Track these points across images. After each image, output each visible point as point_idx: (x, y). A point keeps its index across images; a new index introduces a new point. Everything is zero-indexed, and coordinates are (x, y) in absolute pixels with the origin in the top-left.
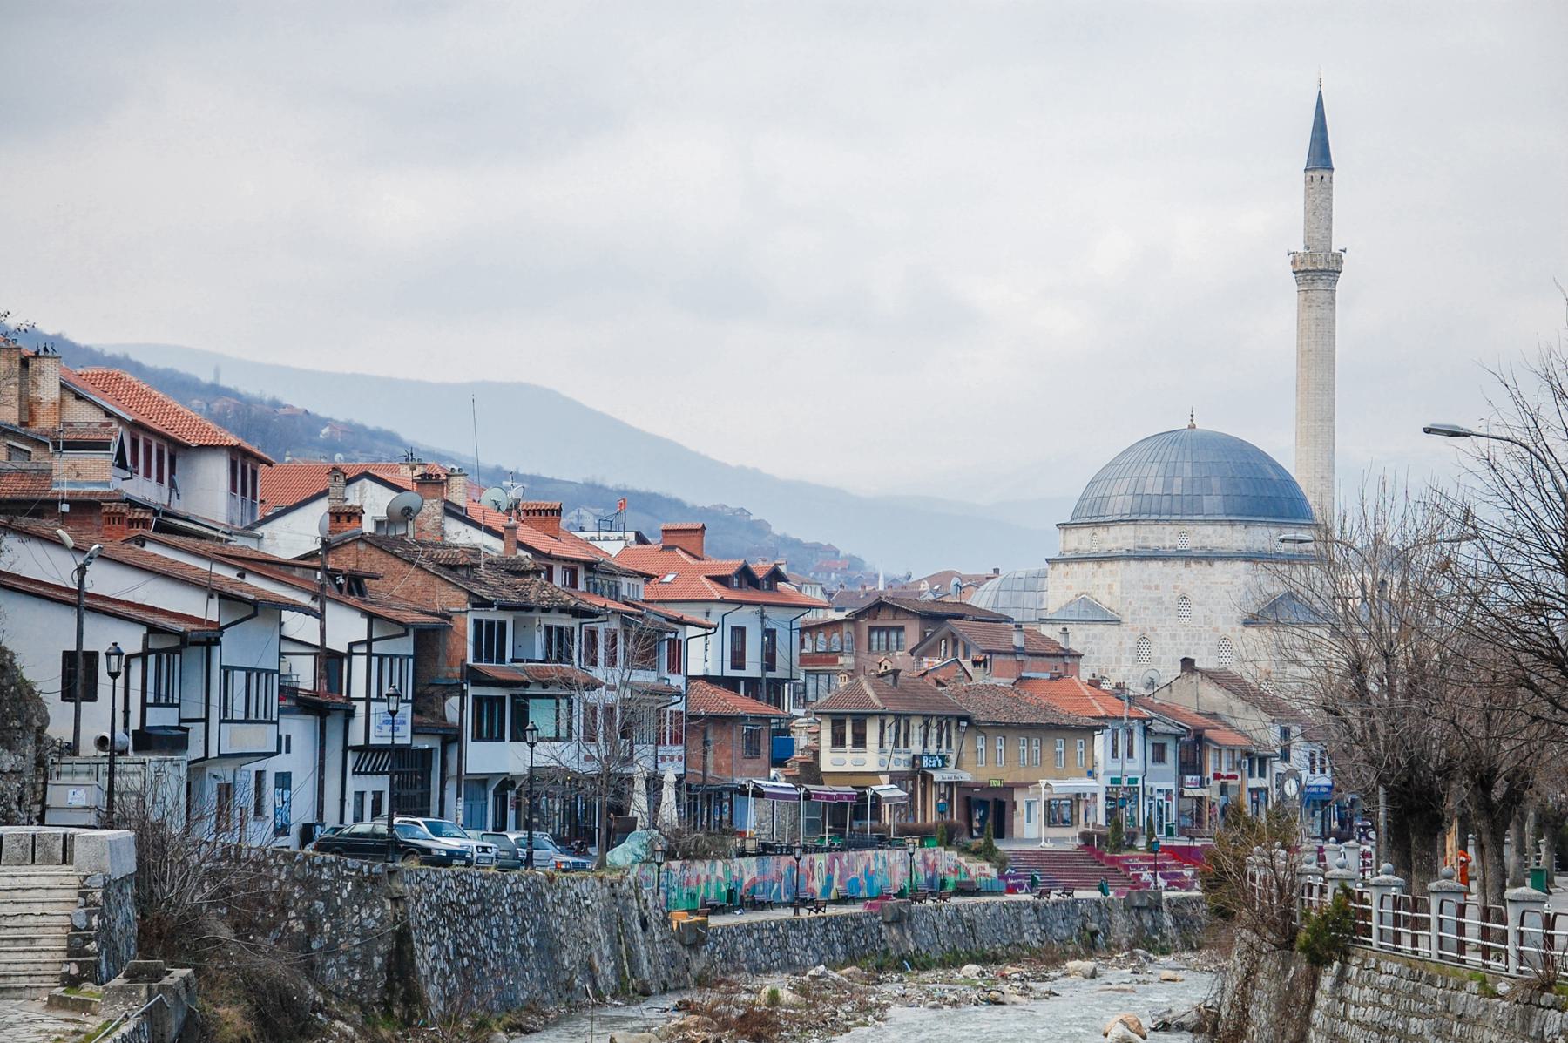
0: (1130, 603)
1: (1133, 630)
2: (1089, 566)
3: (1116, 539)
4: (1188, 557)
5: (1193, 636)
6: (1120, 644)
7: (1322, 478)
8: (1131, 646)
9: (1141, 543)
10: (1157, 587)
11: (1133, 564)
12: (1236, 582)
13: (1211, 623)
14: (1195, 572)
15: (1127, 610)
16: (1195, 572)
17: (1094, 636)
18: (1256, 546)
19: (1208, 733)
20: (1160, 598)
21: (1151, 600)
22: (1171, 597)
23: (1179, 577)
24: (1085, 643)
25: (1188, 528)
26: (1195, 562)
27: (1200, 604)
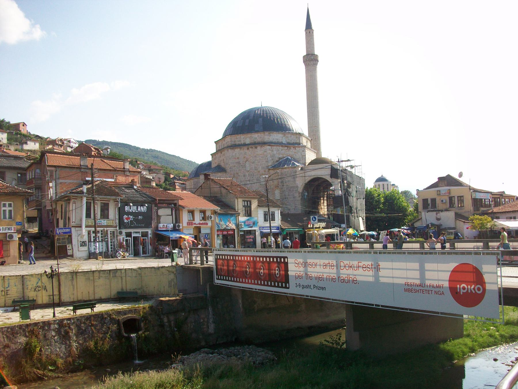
1: (230, 174)
2: (219, 154)
3: (226, 143)
5: (251, 175)
9: (233, 143)
10: (238, 158)
11: (230, 150)
12: (265, 153)
13: (257, 169)
14: (251, 151)
16: (251, 151)
18: (274, 141)
19: (181, 203)
20: (239, 162)
21: (236, 163)
22: (243, 161)
23: (245, 153)
26: (252, 148)
27: (253, 163)
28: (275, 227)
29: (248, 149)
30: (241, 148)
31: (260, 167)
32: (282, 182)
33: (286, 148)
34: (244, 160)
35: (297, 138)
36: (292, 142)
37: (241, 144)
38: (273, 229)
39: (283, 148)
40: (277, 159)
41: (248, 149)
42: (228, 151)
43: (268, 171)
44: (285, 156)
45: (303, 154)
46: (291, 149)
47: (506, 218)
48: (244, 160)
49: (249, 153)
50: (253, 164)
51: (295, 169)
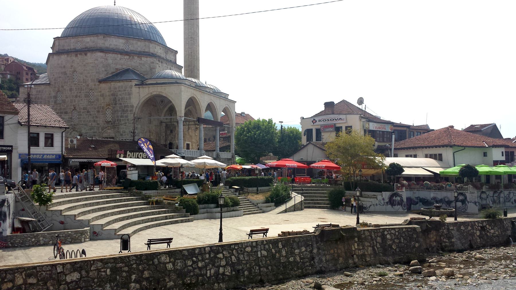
0: (54, 75)
4: (77, 52)
5: (79, 89)
6: (50, 94)
7: (191, 38)
8: (54, 95)
10: (64, 67)
12: (96, 62)
15: (53, 79)
17: (40, 91)
18: (111, 47)
21: (62, 73)
24: (36, 95)
25: (80, 39)
26: (80, 54)
27: (81, 74)
28: (53, 155)
29: (76, 55)
30: (68, 55)
31: (90, 80)
32: (115, 99)
33: (128, 57)
34: (70, 70)
35: (145, 46)
36: (139, 49)
37: (71, 49)
38: (48, 157)
39: (123, 57)
40: (113, 70)
41: (76, 55)
42: (53, 57)
43: (99, 85)
44: (125, 67)
45: (151, 67)
46: (133, 58)
47: (405, 156)
48: (70, 70)
49: (77, 60)
50: (81, 75)
51: (130, 83)
